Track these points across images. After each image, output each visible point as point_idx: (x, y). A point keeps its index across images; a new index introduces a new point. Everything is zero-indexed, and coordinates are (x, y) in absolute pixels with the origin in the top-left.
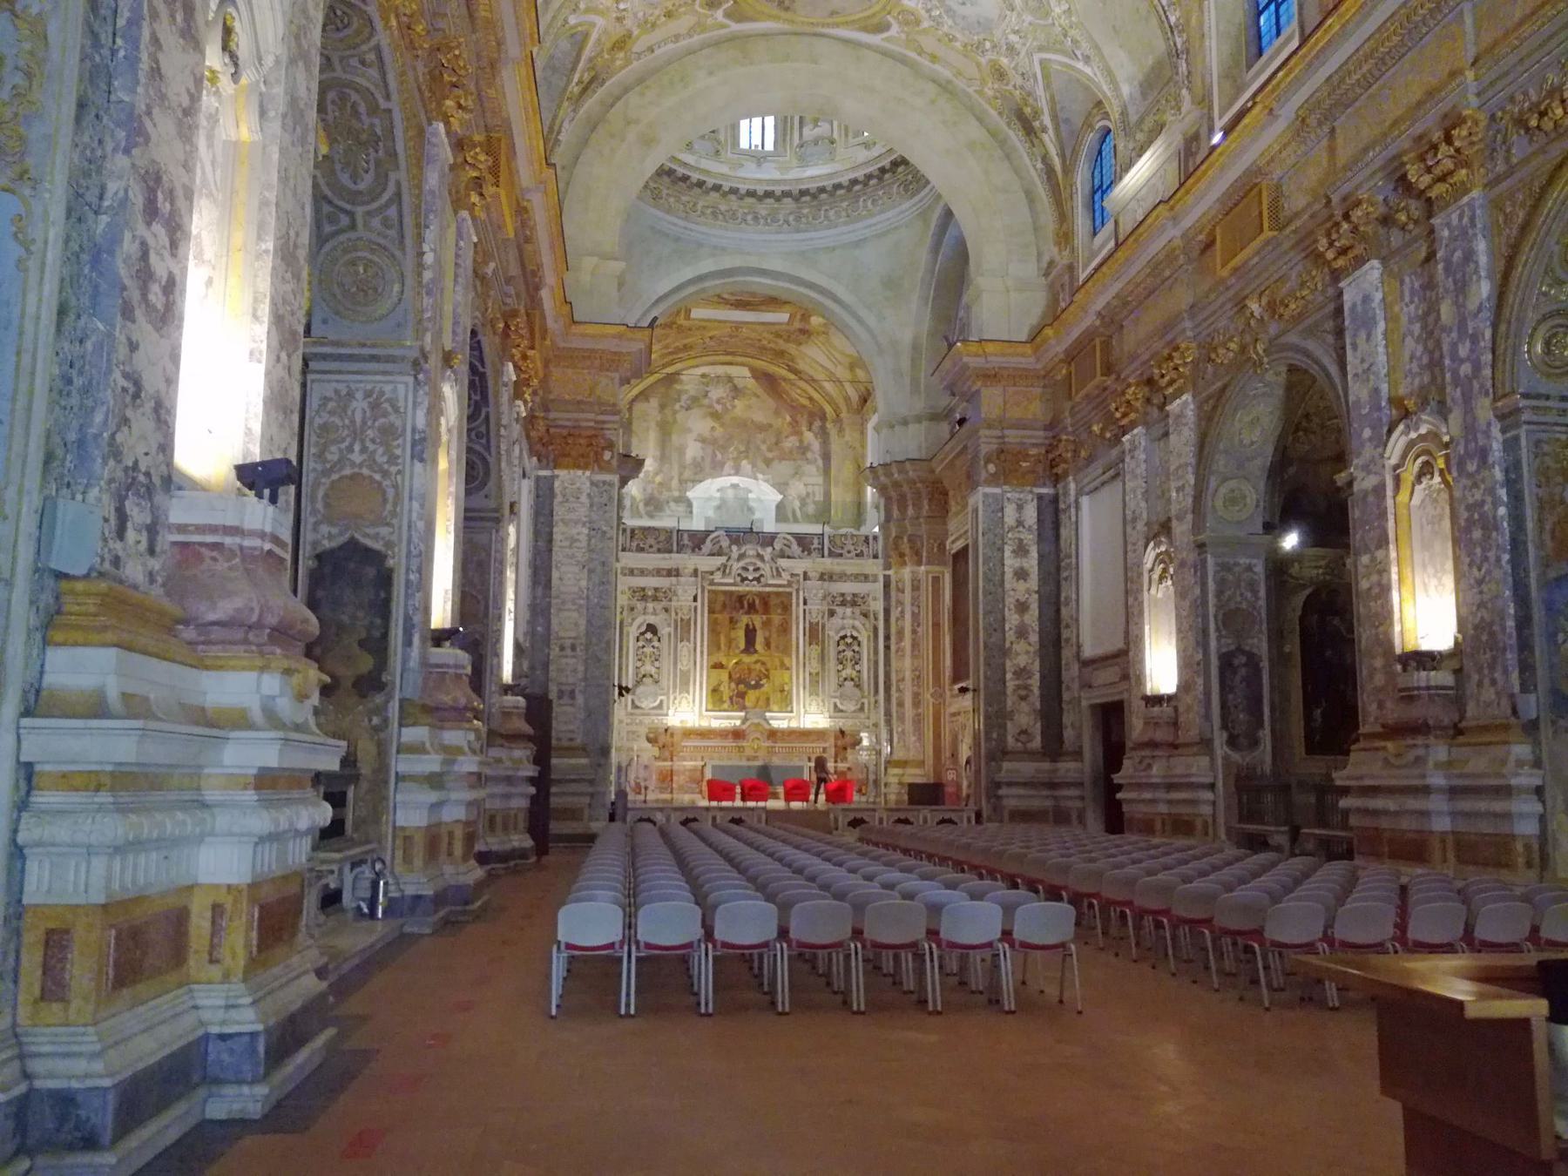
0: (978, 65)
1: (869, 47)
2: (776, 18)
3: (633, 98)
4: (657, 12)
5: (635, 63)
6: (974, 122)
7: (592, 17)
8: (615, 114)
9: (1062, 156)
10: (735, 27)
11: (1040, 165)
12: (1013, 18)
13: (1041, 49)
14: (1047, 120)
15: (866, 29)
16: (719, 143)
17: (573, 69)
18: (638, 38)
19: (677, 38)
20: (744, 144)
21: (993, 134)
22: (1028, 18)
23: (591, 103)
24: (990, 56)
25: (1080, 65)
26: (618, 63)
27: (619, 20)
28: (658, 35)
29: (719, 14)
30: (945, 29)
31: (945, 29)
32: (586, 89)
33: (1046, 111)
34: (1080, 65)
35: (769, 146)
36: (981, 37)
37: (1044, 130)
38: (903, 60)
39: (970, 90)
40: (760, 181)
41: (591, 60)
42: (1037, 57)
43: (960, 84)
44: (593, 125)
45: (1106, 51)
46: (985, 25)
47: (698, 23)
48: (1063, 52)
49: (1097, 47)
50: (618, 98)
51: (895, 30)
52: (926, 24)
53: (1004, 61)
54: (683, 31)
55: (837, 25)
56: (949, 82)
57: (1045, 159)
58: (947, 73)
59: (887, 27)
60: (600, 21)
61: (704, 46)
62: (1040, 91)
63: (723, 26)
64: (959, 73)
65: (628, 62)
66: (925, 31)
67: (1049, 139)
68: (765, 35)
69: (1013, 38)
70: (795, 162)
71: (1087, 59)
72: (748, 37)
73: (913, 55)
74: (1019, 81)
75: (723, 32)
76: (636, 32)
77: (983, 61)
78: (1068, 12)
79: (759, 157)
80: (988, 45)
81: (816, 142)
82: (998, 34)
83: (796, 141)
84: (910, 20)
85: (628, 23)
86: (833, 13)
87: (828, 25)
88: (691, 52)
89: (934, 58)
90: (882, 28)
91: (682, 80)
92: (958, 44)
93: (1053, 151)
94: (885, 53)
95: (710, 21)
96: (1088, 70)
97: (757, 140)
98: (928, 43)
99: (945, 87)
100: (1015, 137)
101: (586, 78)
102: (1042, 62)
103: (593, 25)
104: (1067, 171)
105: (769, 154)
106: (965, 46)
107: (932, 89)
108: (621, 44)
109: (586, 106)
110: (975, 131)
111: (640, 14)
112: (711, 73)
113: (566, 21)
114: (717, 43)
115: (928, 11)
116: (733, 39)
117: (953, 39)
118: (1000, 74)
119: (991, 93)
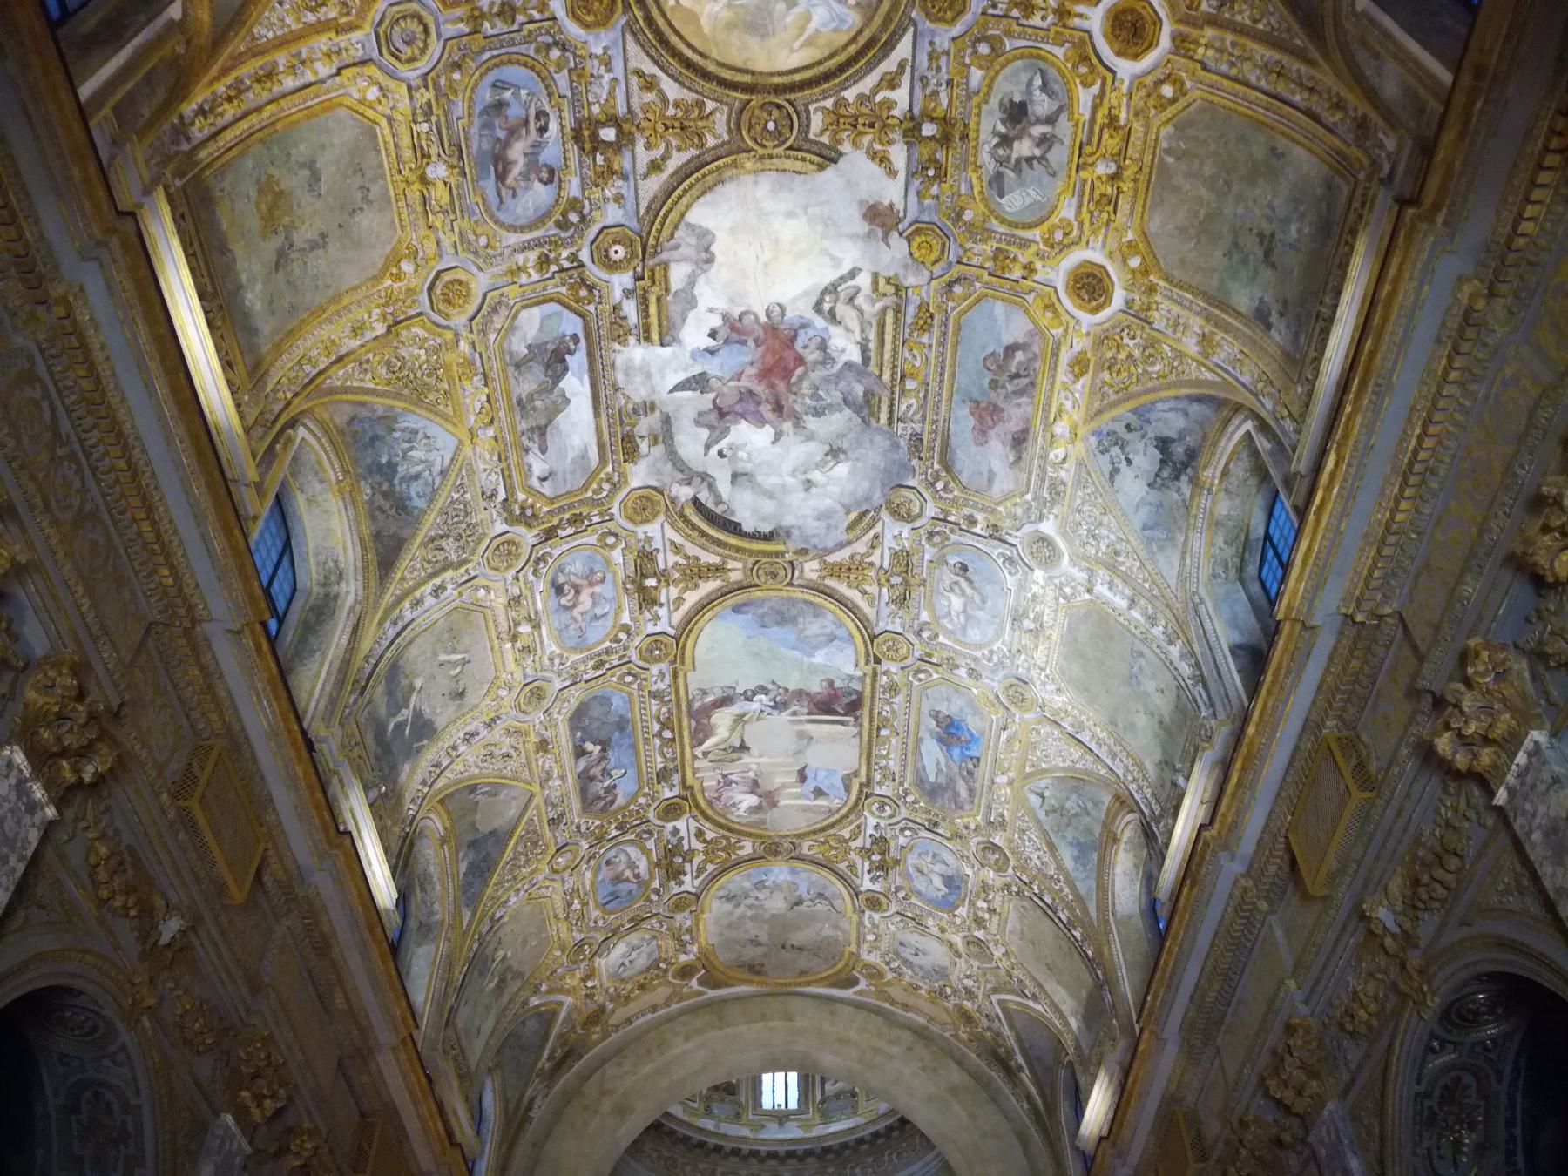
0: (946, 1010)
1: (842, 1001)
2: (751, 982)
3: (610, 1070)
4: (629, 987)
5: (614, 1036)
6: (954, 1066)
7: (560, 997)
8: (591, 1087)
9: (1042, 1094)
10: (712, 993)
11: (1026, 1106)
12: (961, 963)
13: (995, 990)
14: (1021, 1061)
15: (834, 985)
16: (739, 1104)
17: (542, 1047)
18: (613, 1011)
19: (654, 1008)
20: (767, 1103)
21: (977, 1077)
22: (976, 964)
23: (566, 1078)
24: (953, 1001)
25: (1030, 1003)
26: (595, 1037)
27: (590, 996)
28: (633, 1008)
29: (694, 983)
30: (907, 979)
31: (907, 979)
32: (560, 1065)
33: (1017, 1050)
34: (1030, 1003)
35: (793, 1105)
36: (942, 983)
37: (1020, 1069)
38: (877, 1011)
39: (947, 1035)
40: (782, 1142)
41: (561, 1036)
42: (994, 998)
43: (935, 1028)
44: (567, 1098)
45: (1048, 987)
46: (941, 973)
47: (675, 993)
48: (1012, 992)
49: (1040, 985)
50: (596, 1069)
51: (863, 984)
52: (889, 976)
53: (968, 1004)
54: (660, 1002)
55: (808, 984)
56: (926, 1028)
57: (1029, 1097)
58: (922, 1021)
59: (855, 982)
60: (568, 1000)
61: (682, 1013)
62: (1007, 1032)
63: (700, 993)
64: (931, 1019)
65: (606, 1035)
66: (889, 983)
67: (1025, 1076)
68: (739, 999)
69: (969, 983)
70: (818, 1119)
71: (1035, 998)
72: (724, 1001)
73: (886, 1005)
74: (985, 1022)
75: (700, 998)
76: (610, 1006)
77: (949, 1005)
78: (1006, 954)
79: (781, 1116)
80: (949, 991)
81: (837, 1096)
82: (954, 978)
83: (819, 1097)
84: (875, 974)
85: (599, 999)
86: (803, 973)
87: (800, 984)
88: (669, 1019)
89: (905, 1007)
90: (851, 982)
91: (659, 1047)
92: (923, 992)
93: (1033, 1090)
94: (859, 1006)
95: (685, 990)
96: (1039, 1007)
97: (780, 1100)
98: (897, 993)
99: (922, 1034)
100: (997, 1077)
101: (559, 1053)
102: (1000, 1002)
103: (561, 1004)
104: (1051, 1108)
105: (794, 1112)
106: (929, 993)
107: (907, 1036)
108: (597, 1016)
109: (562, 1081)
110: (956, 1076)
111: (611, 990)
112: (687, 1039)
113: (526, 1003)
114: (694, 1010)
115: (888, 964)
116: (710, 1004)
117: (917, 988)
118: (968, 1018)
119: (965, 1036)
